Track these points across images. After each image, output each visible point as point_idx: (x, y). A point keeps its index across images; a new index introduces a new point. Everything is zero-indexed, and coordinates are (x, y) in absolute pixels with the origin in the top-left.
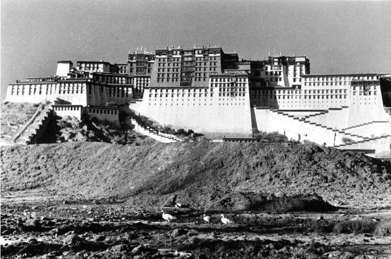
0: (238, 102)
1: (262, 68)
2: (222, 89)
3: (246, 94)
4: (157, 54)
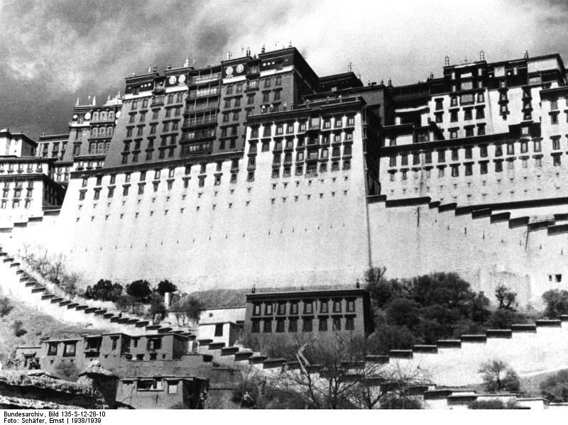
0: (327, 186)
1: (425, 101)
2: (283, 156)
3: (353, 161)
4: (127, 92)
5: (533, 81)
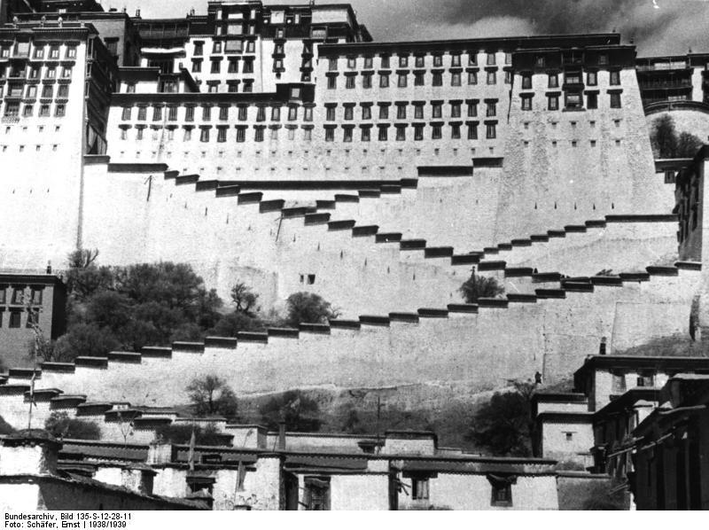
0: (32, 137)
1: (181, 42)
5: (317, 34)
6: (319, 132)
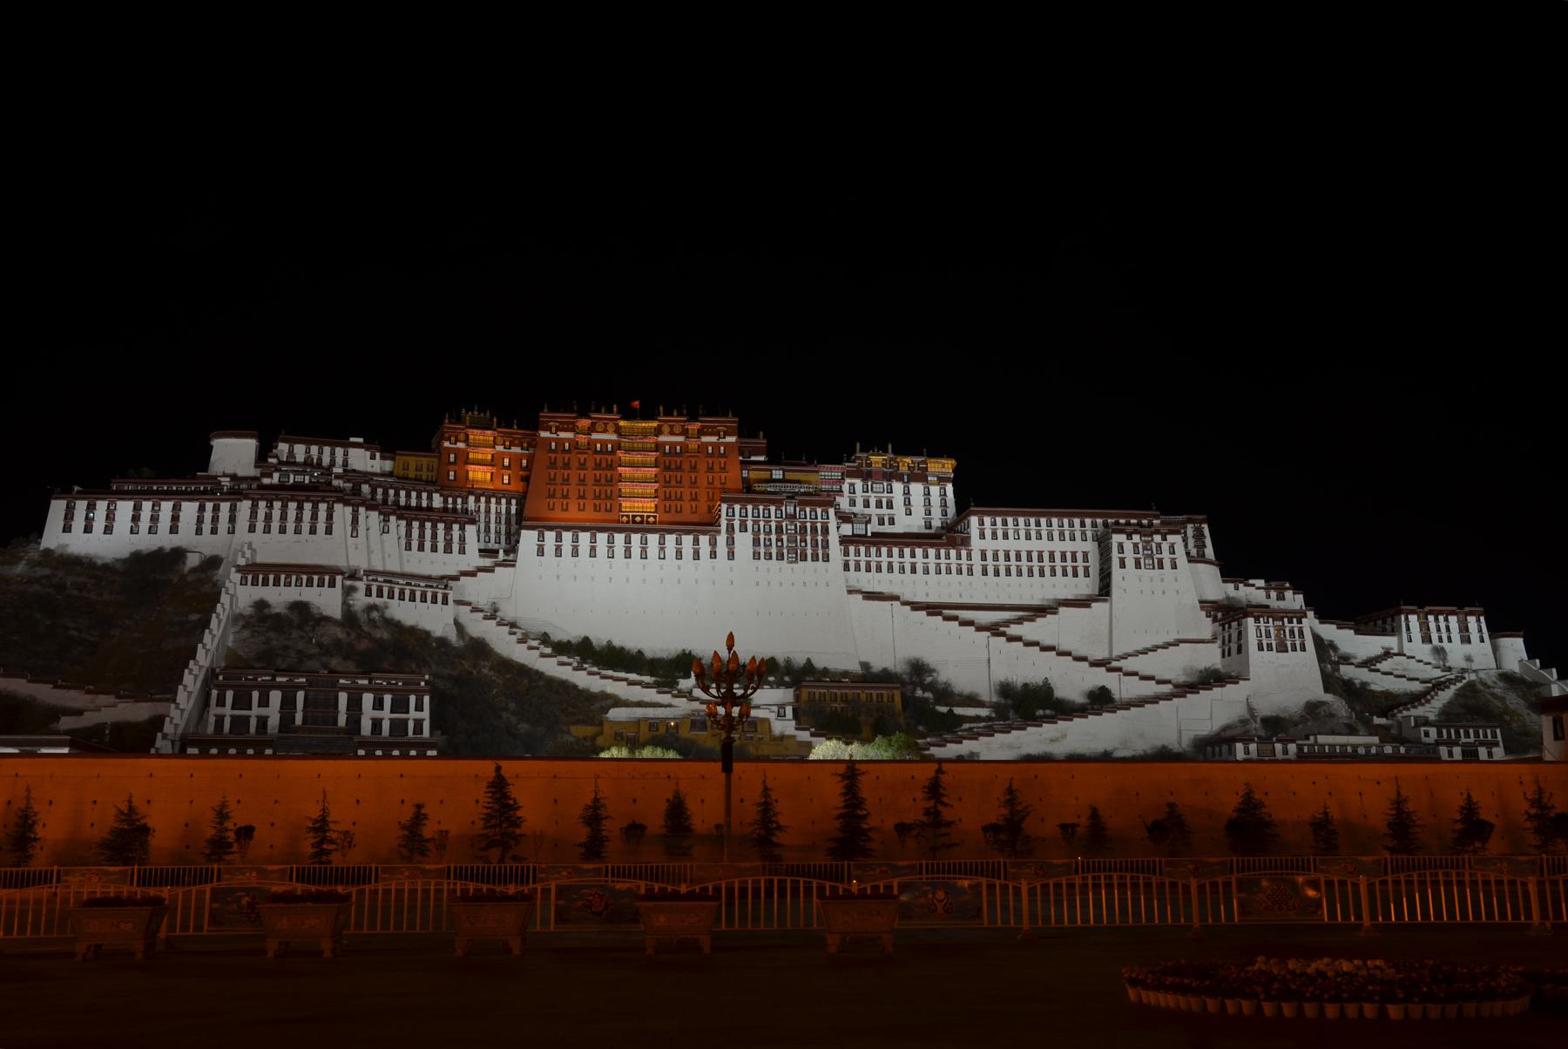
6: (977, 569)
